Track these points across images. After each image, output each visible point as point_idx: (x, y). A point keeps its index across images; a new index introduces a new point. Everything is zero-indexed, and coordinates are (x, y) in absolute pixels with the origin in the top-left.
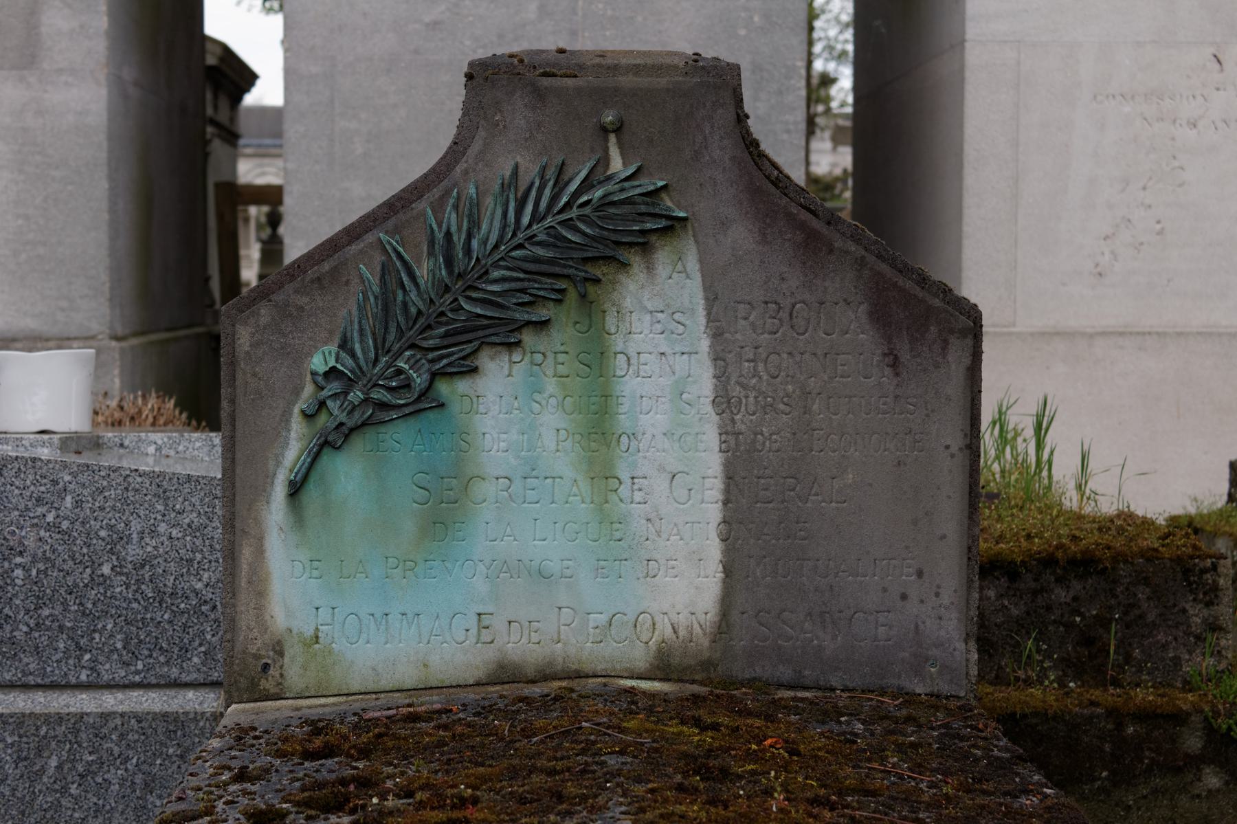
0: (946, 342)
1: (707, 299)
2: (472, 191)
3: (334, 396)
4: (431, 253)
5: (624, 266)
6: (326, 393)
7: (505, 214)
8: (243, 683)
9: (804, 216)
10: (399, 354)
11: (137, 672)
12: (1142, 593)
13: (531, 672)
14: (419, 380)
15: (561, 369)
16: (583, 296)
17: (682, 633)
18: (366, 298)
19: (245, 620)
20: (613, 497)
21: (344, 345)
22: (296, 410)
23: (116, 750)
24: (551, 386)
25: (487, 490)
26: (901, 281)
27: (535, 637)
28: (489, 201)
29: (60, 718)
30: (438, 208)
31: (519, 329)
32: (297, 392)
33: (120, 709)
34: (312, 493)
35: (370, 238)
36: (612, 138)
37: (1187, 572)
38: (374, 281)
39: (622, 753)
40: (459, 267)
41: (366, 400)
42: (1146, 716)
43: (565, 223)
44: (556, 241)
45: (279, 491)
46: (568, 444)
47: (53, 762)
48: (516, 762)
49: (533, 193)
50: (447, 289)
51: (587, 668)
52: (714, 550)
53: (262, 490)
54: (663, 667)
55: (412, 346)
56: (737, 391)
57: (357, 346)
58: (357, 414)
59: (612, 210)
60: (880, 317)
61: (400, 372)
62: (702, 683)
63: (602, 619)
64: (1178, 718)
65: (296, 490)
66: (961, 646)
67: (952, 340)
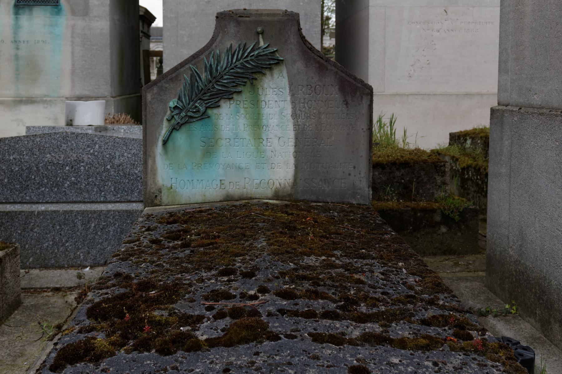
0: (362, 97)
1: (289, 84)
2: (218, 52)
3: (177, 114)
4: (206, 71)
5: (264, 74)
6: (174, 113)
7: (228, 59)
8: (149, 201)
9: (319, 59)
10: (196, 101)
11: (118, 198)
12: (422, 173)
13: (236, 197)
14: (202, 109)
15: (245, 106)
16: (252, 84)
17: (282, 186)
18: (186, 84)
19: (150, 182)
20: (261, 145)
21: (179, 99)
22: (165, 118)
23: (112, 221)
24: (242, 111)
25: (223, 142)
26: (348, 78)
27: (238, 187)
28: (223, 55)
29: (95, 212)
30: (208, 57)
31: (232, 94)
32: (165, 113)
33: (113, 209)
34: (170, 143)
35: (187, 66)
36: (261, 36)
37: (436, 167)
38: (188, 79)
39: (264, 222)
40: (214, 75)
41: (186, 116)
42: (424, 210)
43: (246, 62)
44: (243, 67)
45: (160, 143)
46: (248, 128)
47: (93, 225)
48: (231, 225)
49: (237, 53)
50: (210, 82)
51: (254, 196)
52: (292, 160)
53: (155, 143)
54: (276, 196)
55: (200, 99)
56: (299, 112)
57: (183, 99)
58: (183, 120)
59: (260, 58)
60: (342, 90)
61: (196, 107)
62: (288, 201)
63: (258, 181)
64: (433, 211)
65: (165, 143)
66: (367, 189)
67: (364, 96)
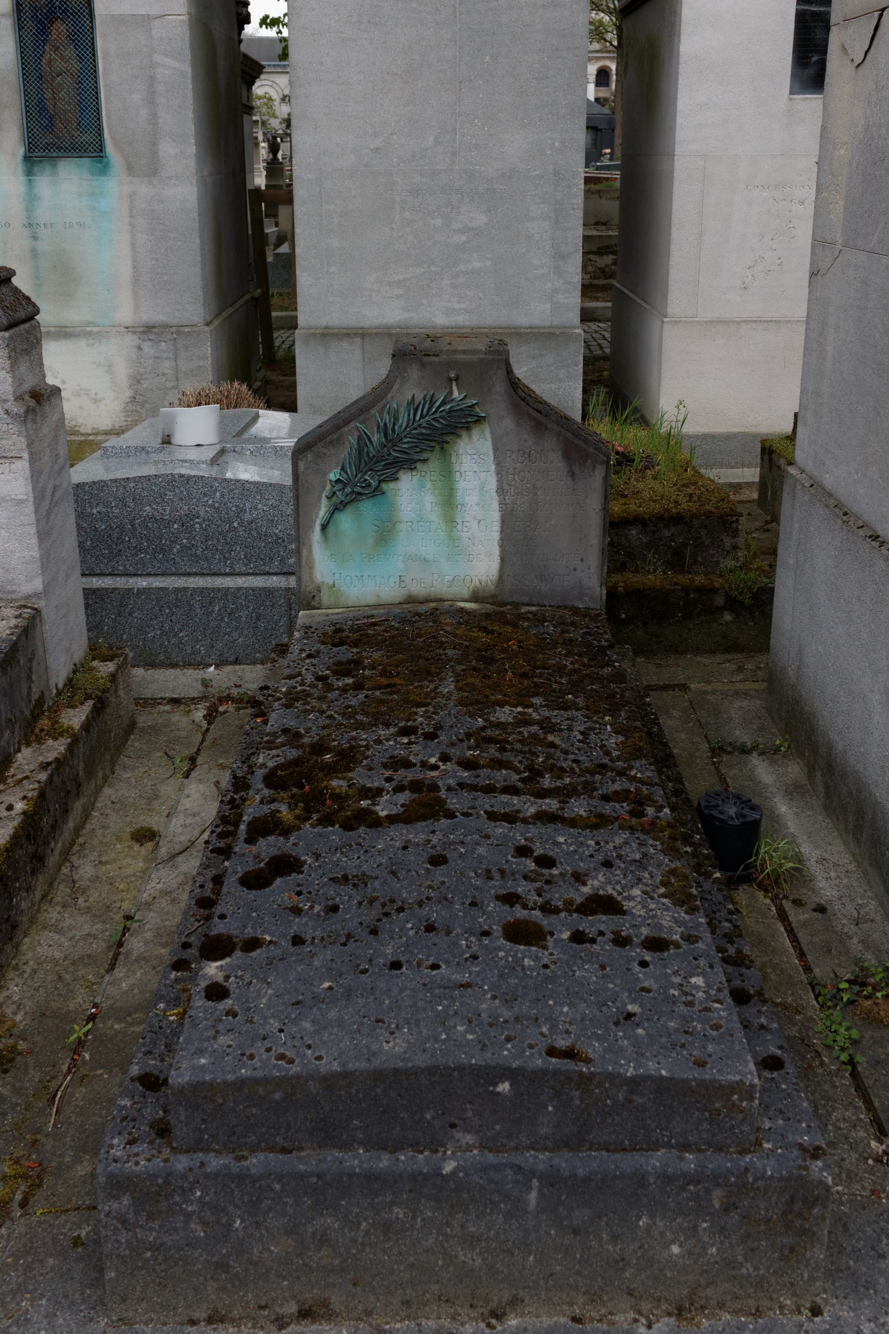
0: (594, 466)
1: (494, 449)
2: (395, 406)
3: (339, 490)
4: (378, 431)
5: (459, 436)
6: (335, 489)
7: (409, 415)
8: (305, 603)
9: (536, 414)
10: (366, 473)
11: (251, 568)
12: (703, 532)
13: (421, 599)
14: (374, 483)
15: (433, 478)
16: (442, 448)
17: (483, 584)
18: (351, 450)
19: (305, 577)
20: (455, 530)
21: (343, 469)
22: (324, 495)
23: (244, 603)
24: (429, 485)
25: (403, 527)
26: (576, 441)
27: (423, 585)
28: (402, 409)
29: (219, 590)
30: (381, 412)
31: (415, 462)
32: (324, 488)
33: (245, 585)
34: (331, 529)
35: (352, 424)
36: (454, 383)
37: (724, 523)
38: (354, 442)
39: (454, 648)
40: (390, 437)
41: (353, 492)
42: (700, 590)
43: (434, 419)
44: (430, 426)
45: (318, 528)
46: (436, 508)
47: (217, 608)
48: (413, 653)
49: (421, 407)
50: (385, 446)
51: (444, 597)
52: (496, 551)
53: (311, 527)
54: (475, 597)
55: (371, 470)
56: (506, 487)
57: (348, 470)
58: (349, 497)
59: (454, 414)
60: (567, 456)
61: (366, 480)
62: (491, 604)
63: (451, 578)
64: (714, 591)
65: (324, 527)
66: (598, 589)
67: (597, 466)
